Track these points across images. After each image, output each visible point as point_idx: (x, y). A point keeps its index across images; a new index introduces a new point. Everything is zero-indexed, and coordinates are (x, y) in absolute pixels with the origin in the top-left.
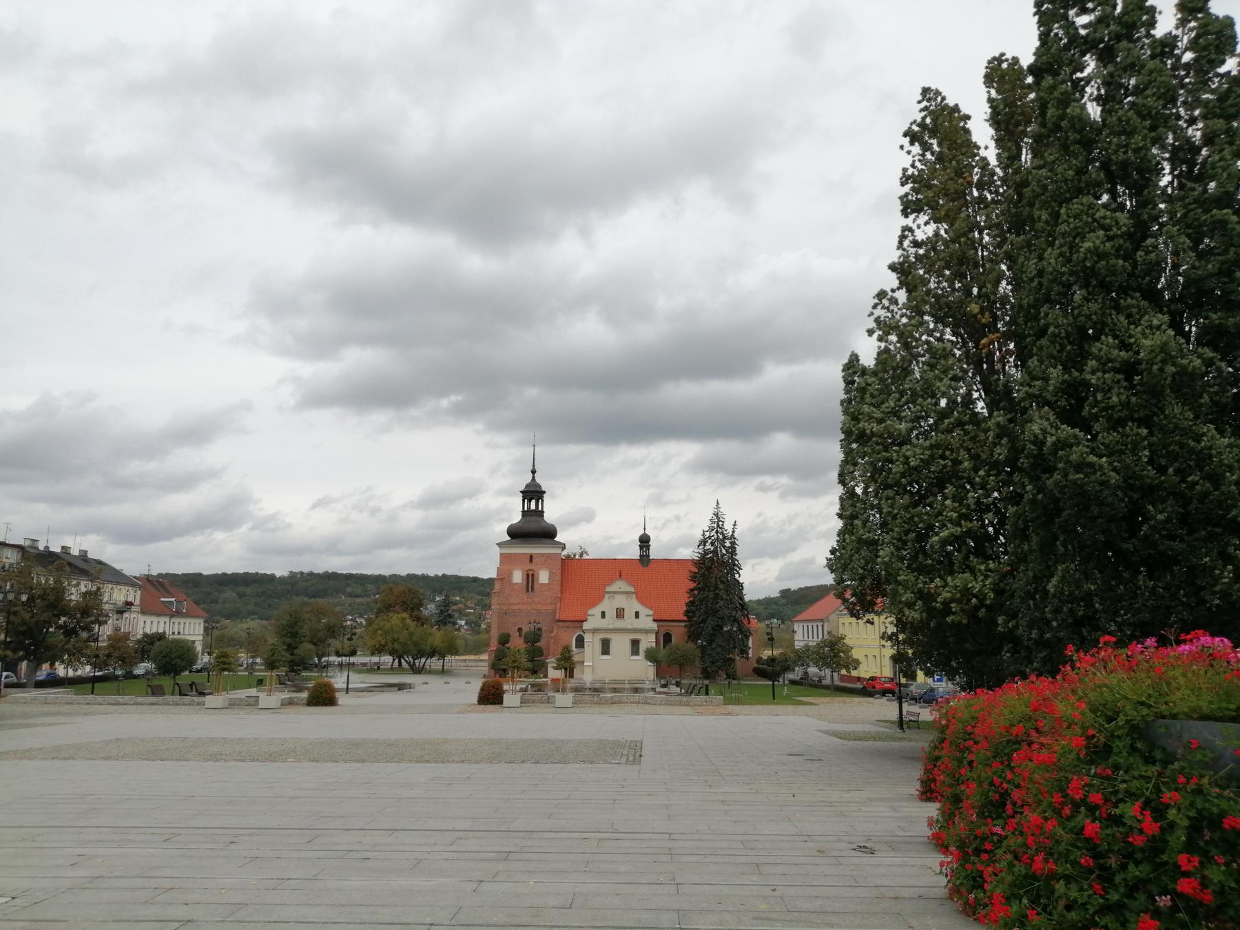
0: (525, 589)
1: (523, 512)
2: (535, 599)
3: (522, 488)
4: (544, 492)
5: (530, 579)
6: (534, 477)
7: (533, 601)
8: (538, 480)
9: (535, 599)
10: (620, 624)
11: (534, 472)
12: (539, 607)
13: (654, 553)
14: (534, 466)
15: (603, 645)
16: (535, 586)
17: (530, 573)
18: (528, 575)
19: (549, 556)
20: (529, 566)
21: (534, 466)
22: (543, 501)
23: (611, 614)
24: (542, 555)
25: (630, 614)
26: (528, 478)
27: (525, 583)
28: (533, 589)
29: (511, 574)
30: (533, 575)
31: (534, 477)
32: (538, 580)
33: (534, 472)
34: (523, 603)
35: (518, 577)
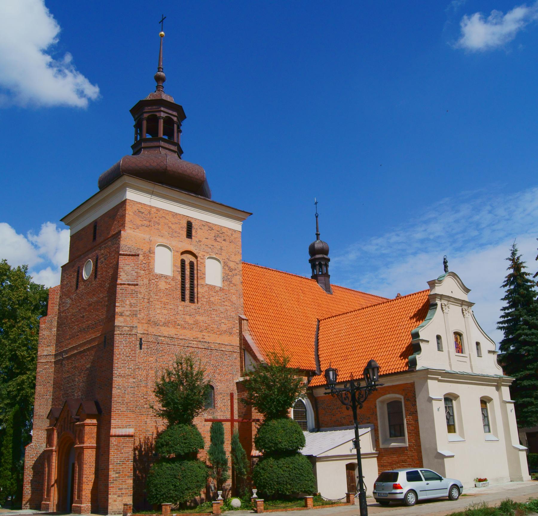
0: (179, 292)
2: (200, 318)
5: (188, 272)
7: (196, 323)
9: (200, 318)
12: (210, 338)
17: (188, 258)
18: (183, 262)
20: (187, 245)
22: (179, 131)
24: (210, 227)
27: (179, 278)
28: (192, 300)
29: (151, 252)
30: (192, 264)
34: (175, 324)
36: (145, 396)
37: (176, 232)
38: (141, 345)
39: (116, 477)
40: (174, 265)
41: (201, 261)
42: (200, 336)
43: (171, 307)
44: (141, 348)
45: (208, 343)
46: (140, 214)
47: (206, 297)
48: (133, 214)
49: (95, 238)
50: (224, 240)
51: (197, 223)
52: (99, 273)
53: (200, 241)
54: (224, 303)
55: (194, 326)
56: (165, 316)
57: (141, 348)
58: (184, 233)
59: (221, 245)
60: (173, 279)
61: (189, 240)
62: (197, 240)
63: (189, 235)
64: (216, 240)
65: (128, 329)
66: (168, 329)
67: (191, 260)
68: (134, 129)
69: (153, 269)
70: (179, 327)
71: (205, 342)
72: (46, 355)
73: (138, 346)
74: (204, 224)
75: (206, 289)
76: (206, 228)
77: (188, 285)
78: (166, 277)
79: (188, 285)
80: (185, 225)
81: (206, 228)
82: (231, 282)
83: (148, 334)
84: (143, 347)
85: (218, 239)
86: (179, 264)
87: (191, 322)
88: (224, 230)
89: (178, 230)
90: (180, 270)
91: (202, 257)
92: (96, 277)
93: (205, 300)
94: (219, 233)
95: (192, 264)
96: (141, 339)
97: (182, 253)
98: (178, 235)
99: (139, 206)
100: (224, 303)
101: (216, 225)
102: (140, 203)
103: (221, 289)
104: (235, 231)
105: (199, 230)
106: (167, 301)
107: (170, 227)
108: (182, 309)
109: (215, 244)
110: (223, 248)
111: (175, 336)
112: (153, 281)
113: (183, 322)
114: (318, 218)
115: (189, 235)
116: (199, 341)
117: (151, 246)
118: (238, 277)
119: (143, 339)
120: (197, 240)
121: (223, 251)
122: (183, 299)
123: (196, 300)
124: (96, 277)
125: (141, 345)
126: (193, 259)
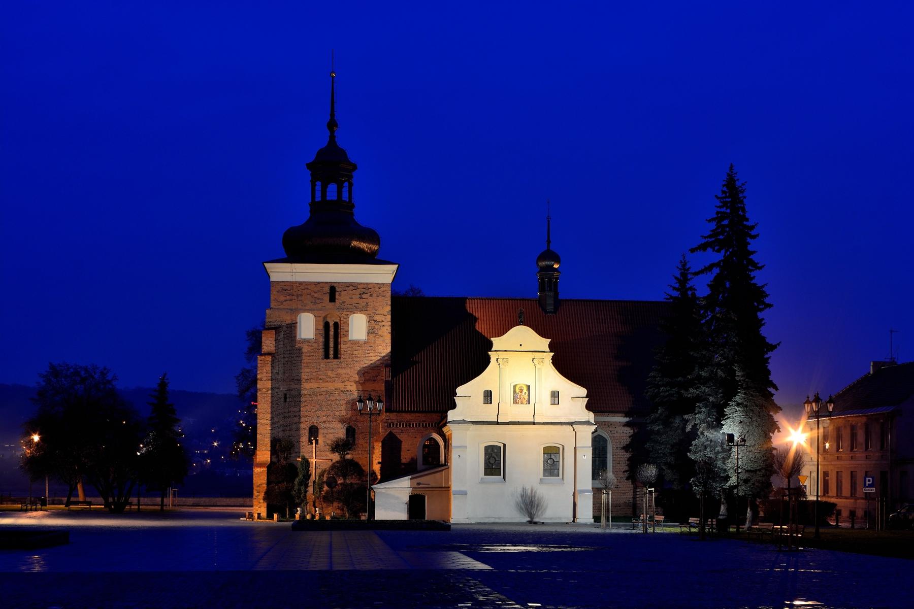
0: (321, 352)
1: (313, 204)
3: (311, 158)
5: (332, 333)
6: (332, 137)
7: (338, 375)
8: (341, 142)
10: (522, 412)
11: (332, 125)
14: (332, 115)
16: (343, 347)
18: (327, 325)
19: (364, 290)
21: (332, 115)
24: (354, 286)
25: (542, 396)
26: (323, 141)
27: (322, 340)
28: (336, 356)
30: (336, 325)
31: (332, 137)
37: (319, 299)
41: (345, 320)
42: (341, 386)
43: (313, 365)
44: (285, 401)
46: (284, 292)
47: (349, 352)
48: (276, 293)
50: (371, 296)
51: (341, 286)
53: (344, 302)
54: (369, 355)
55: (336, 379)
56: (307, 374)
57: (285, 401)
58: (327, 297)
59: (367, 301)
60: (316, 341)
61: (333, 303)
62: (341, 302)
63: (332, 299)
64: (361, 298)
65: (265, 391)
66: (310, 384)
67: (335, 321)
70: (321, 381)
73: (283, 399)
74: (348, 285)
75: (349, 344)
76: (351, 288)
77: (331, 344)
78: (308, 341)
79: (331, 344)
81: (351, 288)
82: (377, 334)
84: (287, 400)
85: (364, 296)
86: (321, 327)
87: (332, 376)
88: (370, 287)
89: (321, 297)
90: (322, 332)
91: (346, 317)
93: (348, 354)
94: (363, 290)
95: (336, 324)
96: (286, 395)
98: (322, 301)
99: (283, 284)
100: (369, 355)
101: (361, 283)
103: (365, 342)
104: (383, 284)
105: (343, 293)
106: (310, 361)
107: (312, 296)
108: (324, 366)
109: (361, 301)
110: (369, 304)
111: (317, 390)
113: (324, 377)
115: (332, 299)
117: (293, 317)
118: (385, 328)
120: (341, 302)
121: (368, 306)
122: (327, 356)
125: (285, 398)
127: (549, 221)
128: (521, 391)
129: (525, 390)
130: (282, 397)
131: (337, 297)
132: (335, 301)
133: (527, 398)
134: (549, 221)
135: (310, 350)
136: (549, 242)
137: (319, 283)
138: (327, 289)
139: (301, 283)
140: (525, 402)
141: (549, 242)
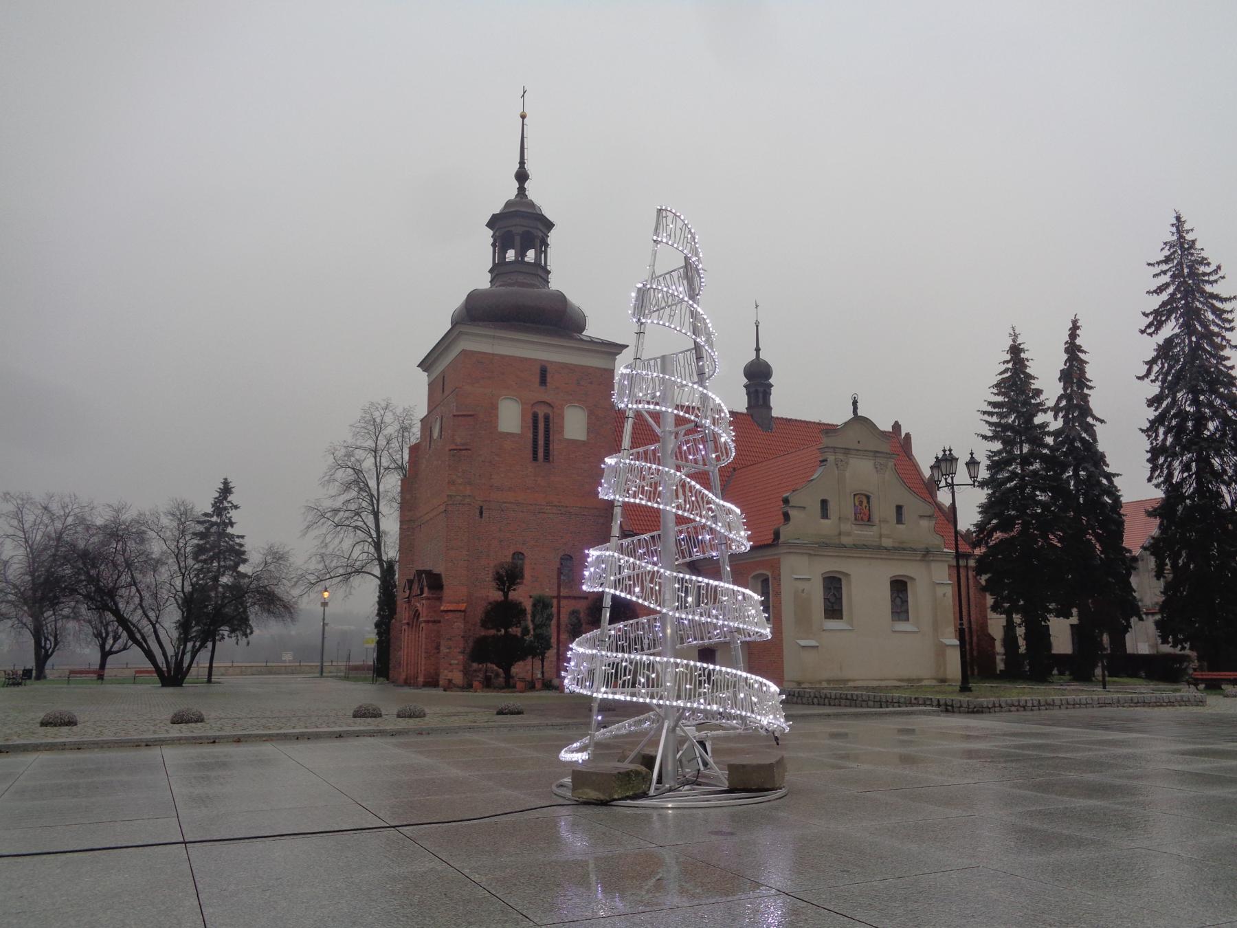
4: (549, 225)
5: (541, 426)
6: (522, 190)
13: (782, 405)
14: (522, 163)
15: (827, 588)
16: (555, 447)
18: (535, 417)
21: (522, 163)
23: (843, 507)
25: (883, 509)
29: (495, 407)
30: (547, 418)
31: (522, 190)
32: (561, 429)
33: (522, 176)
35: (510, 417)
36: (487, 569)
38: (481, 513)
39: (447, 653)
40: (523, 420)
45: (567, 507)
49: (443, 391)
50: (591, 383)
52: (443, 433)
58: (537, 380)
61: (544, 387)
63: (543, 381)
67: (546, 411)
68: (491, 248)
69: (496, 427)
71: (562, 506)
72: (407, 521)
77: (541, 442)
79: (541, 442)
80: (538, 371)
83: (490, 501)
84: (483, 515)
92: (441, 438)
95: (547, 418)
96: (481, 507)
97: (533, 405)
102: (479, 353)
103: (584, 443)
104: (605, 370)
112: (496, 441)
114: (759, 328)
115: (543, 381)
116: (555, 506)
119: (484, 508)
122: (535, 458)
123: (551, 459)
124: (441, 438)
125: (481, 513)
126: (548, 410)
127: (757, 326)
128: (861, 503)
129: (865, 503)
130: (478, 511)
131: (549, 380)
132: (546, 386)
133: (866, 511)
134: (757, 326)
135: (513, 447)
136: (758, 350)
137: (526, 359)
138: (537, 370)
139: (503, 357)
140: (866, 518)
141: (758, 350)
